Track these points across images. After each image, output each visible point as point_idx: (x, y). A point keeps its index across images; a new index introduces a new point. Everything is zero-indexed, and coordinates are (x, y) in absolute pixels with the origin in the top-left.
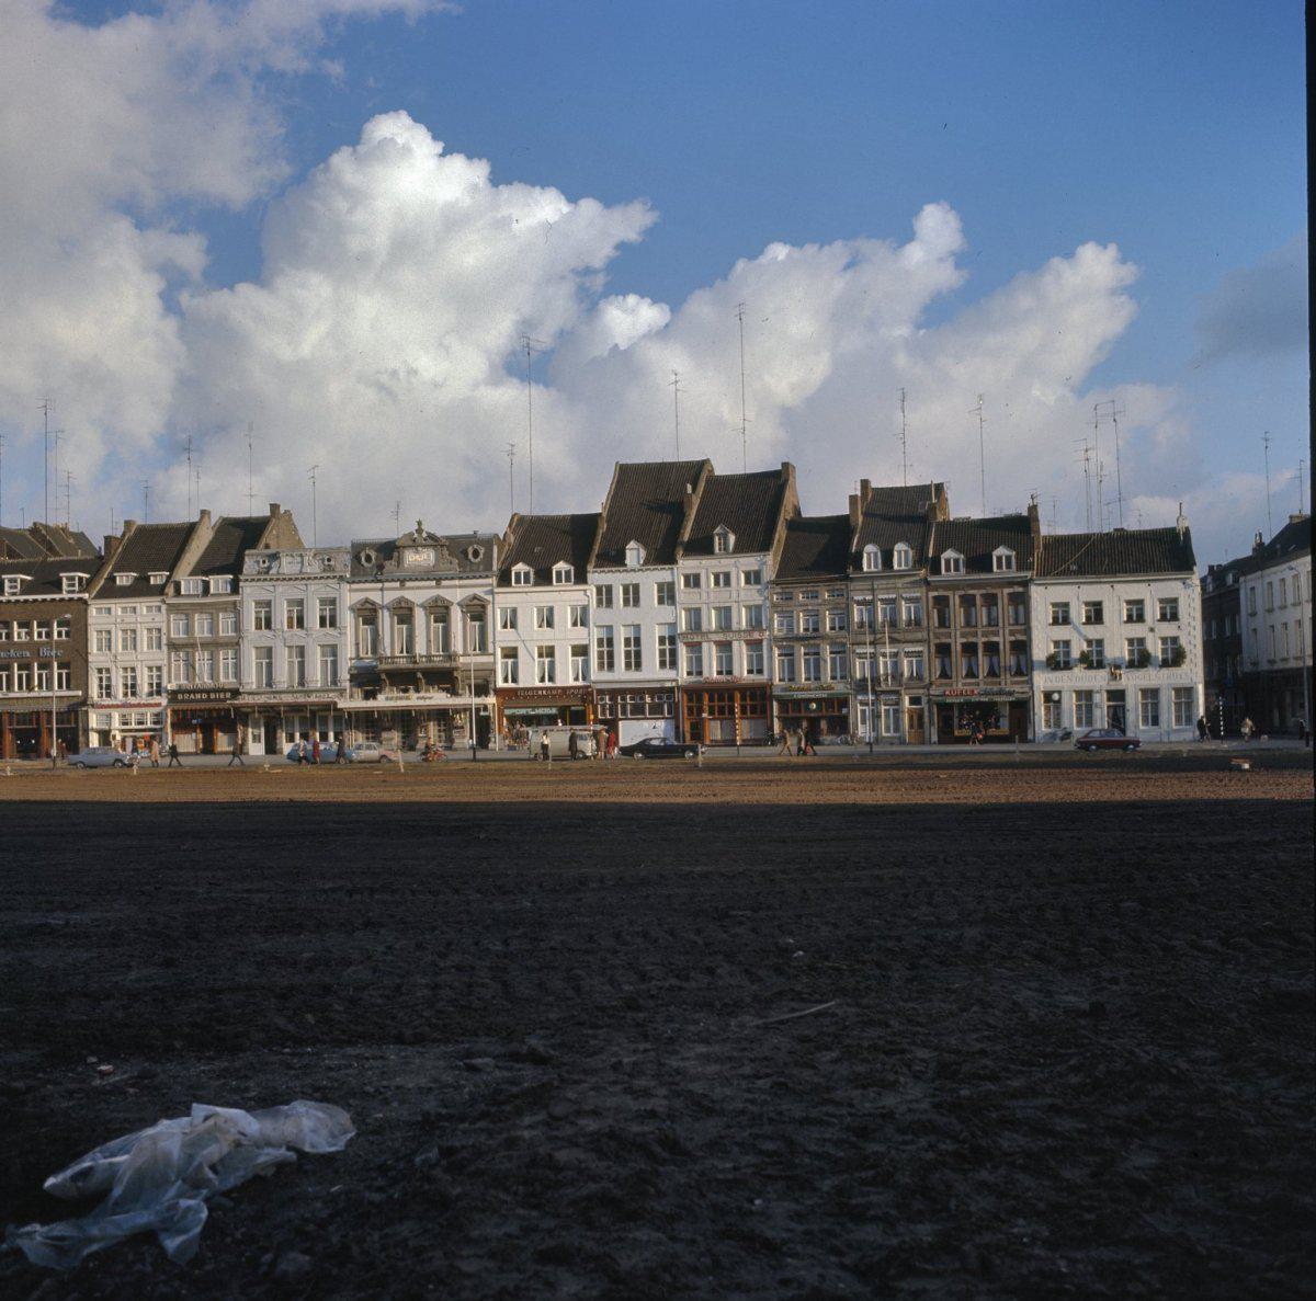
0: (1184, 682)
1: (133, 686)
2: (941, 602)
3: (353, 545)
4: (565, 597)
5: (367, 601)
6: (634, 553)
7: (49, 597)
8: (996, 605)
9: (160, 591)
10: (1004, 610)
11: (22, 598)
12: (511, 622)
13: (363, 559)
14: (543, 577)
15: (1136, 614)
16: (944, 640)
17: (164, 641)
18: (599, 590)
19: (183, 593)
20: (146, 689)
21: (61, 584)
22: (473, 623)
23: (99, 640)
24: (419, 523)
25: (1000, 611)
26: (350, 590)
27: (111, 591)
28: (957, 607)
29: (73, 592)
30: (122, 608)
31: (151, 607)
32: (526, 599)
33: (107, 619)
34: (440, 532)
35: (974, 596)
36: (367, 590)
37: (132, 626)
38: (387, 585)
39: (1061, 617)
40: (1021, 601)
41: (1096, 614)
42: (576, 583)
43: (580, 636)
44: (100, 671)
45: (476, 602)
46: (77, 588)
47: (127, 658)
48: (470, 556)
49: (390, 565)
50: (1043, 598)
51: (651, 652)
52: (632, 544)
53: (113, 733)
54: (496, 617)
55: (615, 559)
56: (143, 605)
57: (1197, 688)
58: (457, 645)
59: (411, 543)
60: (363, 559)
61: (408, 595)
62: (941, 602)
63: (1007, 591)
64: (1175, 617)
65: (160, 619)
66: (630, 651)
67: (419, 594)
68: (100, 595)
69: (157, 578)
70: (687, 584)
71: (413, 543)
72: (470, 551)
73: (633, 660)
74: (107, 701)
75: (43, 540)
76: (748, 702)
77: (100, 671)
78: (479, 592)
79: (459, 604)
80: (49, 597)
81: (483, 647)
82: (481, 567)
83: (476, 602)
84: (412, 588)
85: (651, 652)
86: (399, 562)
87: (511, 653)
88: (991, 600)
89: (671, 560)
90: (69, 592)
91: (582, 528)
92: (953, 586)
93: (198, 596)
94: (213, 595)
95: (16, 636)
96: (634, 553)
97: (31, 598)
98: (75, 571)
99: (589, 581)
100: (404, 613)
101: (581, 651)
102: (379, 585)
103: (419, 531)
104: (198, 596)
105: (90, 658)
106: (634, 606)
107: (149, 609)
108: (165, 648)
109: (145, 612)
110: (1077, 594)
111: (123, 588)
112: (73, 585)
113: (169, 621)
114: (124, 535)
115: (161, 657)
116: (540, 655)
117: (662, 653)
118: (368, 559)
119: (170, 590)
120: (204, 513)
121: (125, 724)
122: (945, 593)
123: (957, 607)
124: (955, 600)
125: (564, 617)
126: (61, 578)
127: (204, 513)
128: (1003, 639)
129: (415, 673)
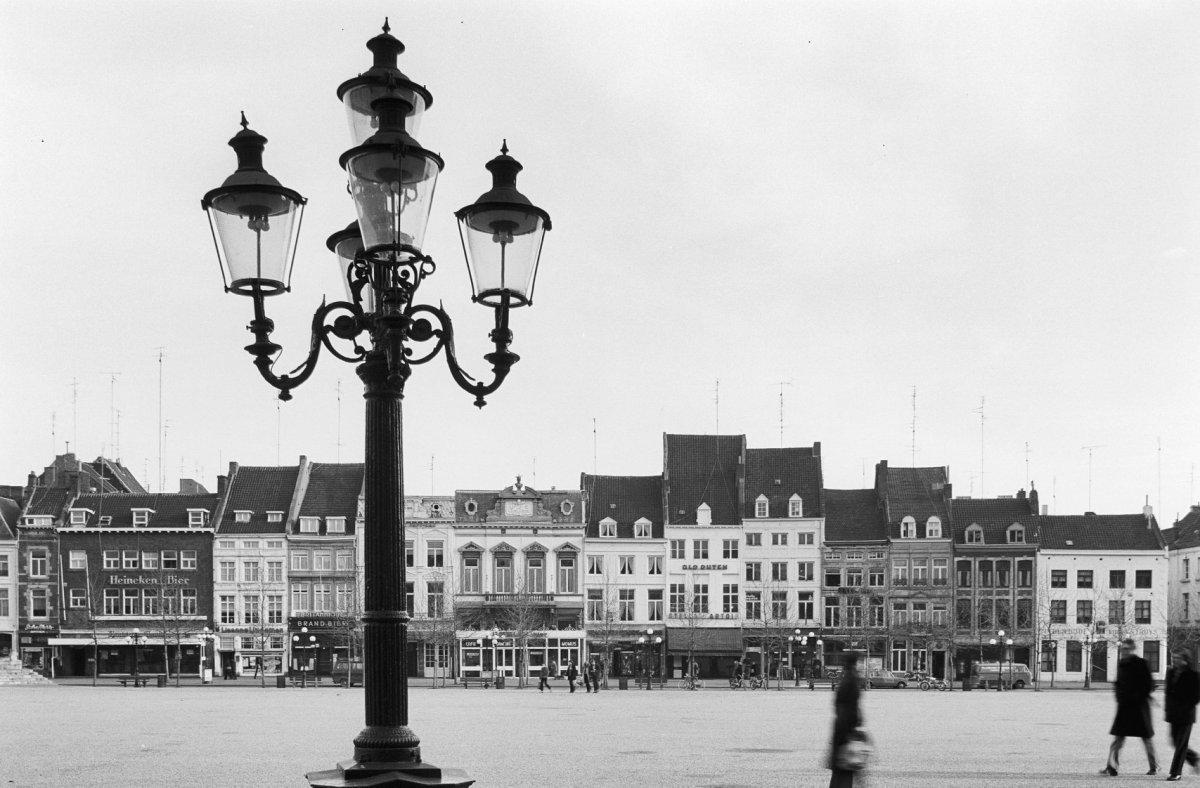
0: (1152, 637)
1: (232, 614)
2: (964, 567)
3: (457, 494)
4: (641, 551)
5: (471, 545)
6: (704, 513)
7: (177, 530)
8: (1009, 571)
9: (280, 528)
10: (1013, 573)
11: (151, 530)
12: (596, 569)
13: (467, 508)
14: (625, 531)
15: (1117, 579)
16: (964, 597)
17: (284, 574)
18: (674, 543)
19: (301, 530)
20: (267, 617)
21: (187, 518)
22: (564, 568)
23: (224, 571)
24: (519, 479)
25: (1012, 574)
26: (457, 535)
27: (230, 527)
28: (977, 572)
29: (197, 526)
30: (245, 543)
31: (249, 543)
32: (611, 552)
33: (229, 551)
34: (541, 486)
35: (992, 562)
36: (471, 535)
37: (255, 560)
38: (489, 531)
39: (1059, 579)
40: (1027, 568)
41: (1086, 580)
42: (654, 536)
43: (655, 582)
44: (224, 598)
45: (568, 549)
46: (202, 523)
47: (272, 587)
48: (467, 510)
49: (492, 515)
50: (1047, 562)
51: (716, 604)
52: (704, 506)
53: (237, 654)
54: (583, 563)
55: (690, 519)
56: (263, 541)
57: (961, 644)
58: (551, 587)
59: (512, 496)
60: (467, 508)
61: (509, 541)
62: (964, 567)
63: (1017, 559)
64: (1089, 585)
65: (282, 553)
66: (698, 597)
67: (519, 542)
68: (224, 530)
69: (274, 517)
70: (750, 543)
71: (511, 495)
72: (467, 505)
73: (701, 604)
74: (229, 626)
75: (107, 473)
76: (559, 648)
77: (224, 598)
78: (572, 541)
79: (555, 551)
80: (177, 530)
81: (572, 587)
82: (572, 520)
83: (568, 549)
84: (515, 535)
85: (716, 604)
86: (501, 510)
87: (596, 595)
88: (1004, 567)
89: (737, 521)
90: (193, 526)
91: (650, 485)
92: (975, 553)
93: (315, 534)
94: (329, 534)
95: (105, 563)
96: (704, 513)
97: (118, 530)
98: (82, 507)
99: (666, 536)
100: (503, 556)
101: (655, 594)
102: (483, 531)
103: (519, 486)
104: (315, 534)
105: (216, 587)
106: (733, 557)
107: (270, 544)
108: (285, 579)
109: (268, 549)
110: (1072, 562)
111: (241, 524)
112: (199, 520)
113: (289, 557)
114: (230, 475)
115: (283, 587)
116: (622, 597)
117: (726, 599)
118: (471, 507)
119: (289, 527)
120: (303, 458)
121: (246, 646)
122: (968, 559)
123: (977, 572)
124: (975, 564)
125: (642, 566)
126: (187, 513)
127: (303, 458)
128: (1013, 597)
129: (549, 610)
